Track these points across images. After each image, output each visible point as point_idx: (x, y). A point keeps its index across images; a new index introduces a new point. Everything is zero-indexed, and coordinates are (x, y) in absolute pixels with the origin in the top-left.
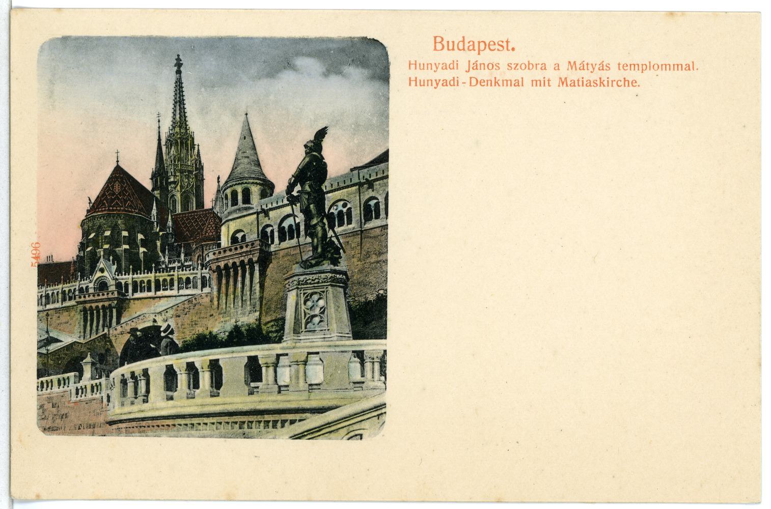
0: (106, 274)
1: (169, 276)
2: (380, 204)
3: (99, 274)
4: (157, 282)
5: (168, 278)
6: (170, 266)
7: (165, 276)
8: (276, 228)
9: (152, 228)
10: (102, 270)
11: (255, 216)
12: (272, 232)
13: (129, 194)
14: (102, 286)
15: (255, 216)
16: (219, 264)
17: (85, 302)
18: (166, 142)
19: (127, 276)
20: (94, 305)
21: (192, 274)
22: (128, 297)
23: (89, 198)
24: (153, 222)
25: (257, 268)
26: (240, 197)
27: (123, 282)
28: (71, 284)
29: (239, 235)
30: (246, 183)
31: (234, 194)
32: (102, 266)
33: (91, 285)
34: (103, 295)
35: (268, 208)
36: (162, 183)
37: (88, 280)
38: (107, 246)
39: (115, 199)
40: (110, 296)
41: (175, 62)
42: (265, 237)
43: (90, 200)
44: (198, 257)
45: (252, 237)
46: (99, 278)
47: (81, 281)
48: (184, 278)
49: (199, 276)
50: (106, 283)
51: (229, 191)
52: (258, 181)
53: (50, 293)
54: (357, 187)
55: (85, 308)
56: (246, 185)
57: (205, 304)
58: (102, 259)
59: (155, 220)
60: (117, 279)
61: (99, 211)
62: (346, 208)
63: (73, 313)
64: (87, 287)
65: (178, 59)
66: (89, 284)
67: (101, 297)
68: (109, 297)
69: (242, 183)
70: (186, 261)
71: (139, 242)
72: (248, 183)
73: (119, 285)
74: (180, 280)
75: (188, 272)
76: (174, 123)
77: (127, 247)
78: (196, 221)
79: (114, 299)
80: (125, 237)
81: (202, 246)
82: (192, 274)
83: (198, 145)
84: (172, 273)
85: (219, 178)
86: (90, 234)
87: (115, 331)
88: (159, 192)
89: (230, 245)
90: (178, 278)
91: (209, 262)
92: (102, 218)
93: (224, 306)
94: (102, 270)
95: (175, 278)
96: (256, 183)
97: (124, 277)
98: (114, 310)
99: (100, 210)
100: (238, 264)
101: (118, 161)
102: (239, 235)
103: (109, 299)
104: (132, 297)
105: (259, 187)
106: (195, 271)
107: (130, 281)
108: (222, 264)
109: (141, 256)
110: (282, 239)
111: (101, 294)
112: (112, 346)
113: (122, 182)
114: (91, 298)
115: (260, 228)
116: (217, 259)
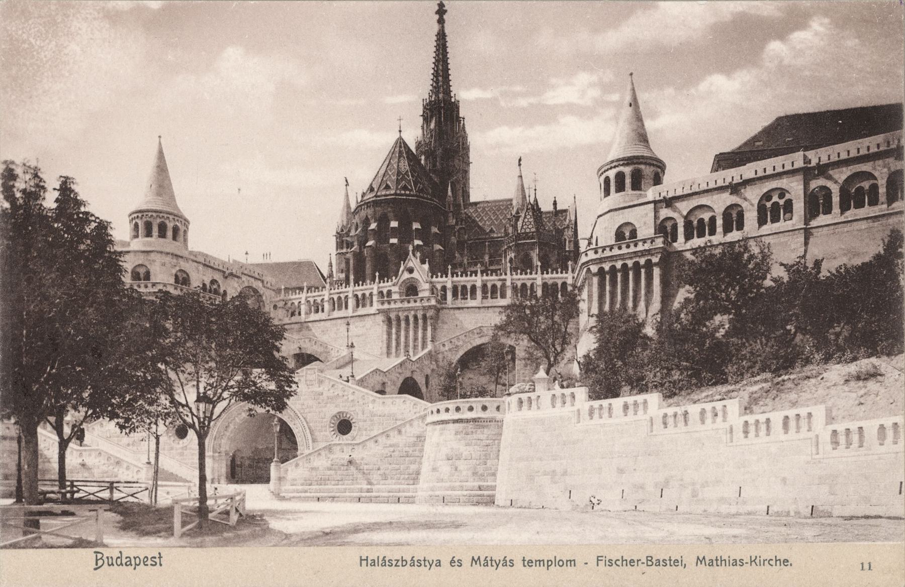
0: (415, 275)
1: (500, 280)
3: (406, 275)
4: (484, 286)
5: (499, 284)
6: (491, 268)
7: (494, 280)
9: (447, 220)
10: (411, 271)
11: (652, 205)
12: (675, 227)
13: (418, 175)
14: (411, 290)
15: (652, 205)
16: (603, 265)
18: (424, 112)
23: (347, 181)
25: (657, 272)
26: (628, 181)
28: (364, 287)
32: (410, 264)
33: (395, 289)
34: (415, 301)
37: (390, 283)
41: (437, 8)
43: (347, 181)
44: (511, 259)
45: (646, 230)
47: (380, 283)
48: (519, 284)
50: (416, 287)
51: (612, 174)
59: (452, 209)
60: (431, 283)
62: (771, 202)
64: (389, 293)
65: (441, 5)
66: (392, 286)
67: (412, 304)
70: (491, 263)
73: (433, 290)
76: (435, 87)
77: (420, 243)
78: (487, 213)
79: (430, 307)
83: (464, 118)
84: (503, 277)
85: (520, 160)
86: (370, 225)
94: (411, 271)
95: (508, 283)
97: (439, 279)
104: (451, 306)
106: (534, 276)
108: (607, 267)
110: (688, 237)
114: (399, 305)
116: (600, 259)
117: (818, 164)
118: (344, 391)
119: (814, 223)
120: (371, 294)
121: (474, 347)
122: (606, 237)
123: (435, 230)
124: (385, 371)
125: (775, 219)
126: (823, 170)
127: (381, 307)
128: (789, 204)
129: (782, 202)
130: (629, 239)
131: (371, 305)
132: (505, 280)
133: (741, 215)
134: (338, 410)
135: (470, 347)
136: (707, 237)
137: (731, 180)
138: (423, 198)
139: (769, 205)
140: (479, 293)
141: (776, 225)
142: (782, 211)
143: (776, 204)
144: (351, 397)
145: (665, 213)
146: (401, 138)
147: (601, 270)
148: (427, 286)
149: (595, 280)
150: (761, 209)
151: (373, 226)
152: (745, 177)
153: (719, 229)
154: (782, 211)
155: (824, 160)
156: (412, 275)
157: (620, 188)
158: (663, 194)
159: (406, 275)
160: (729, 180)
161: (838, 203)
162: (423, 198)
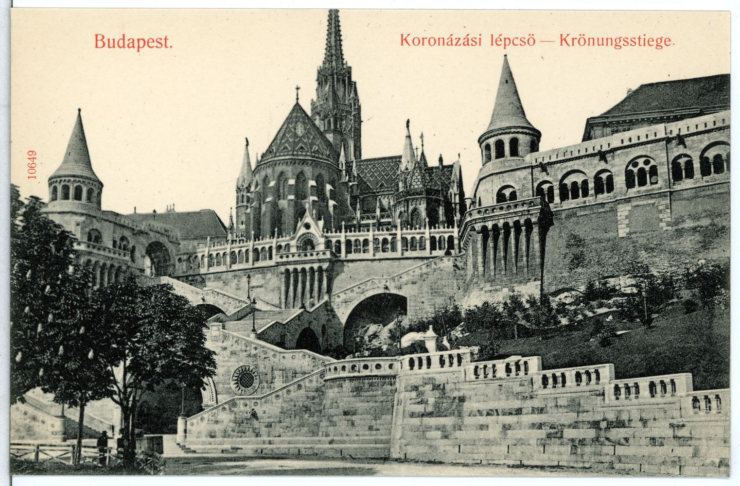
0: (312, 230)
1: (390, 234)
2: (694, 162)
3: (303, 230)
7: (386, 234)
8: (556, 185)
10: (307, 226)
12: (551, 189)
14: (308, 243)
15: (530, 170)
16: (486, 224)
17: (288, 263)
19: (338, 234)
20: (299, 267)
21: (438, 233)
22: (341, 259)
23: (247, 141)
24: (341, 171)
25: (536, 230)
27: (334, 240)
29: (507, 192)
30: (514, 132)
31: (500, 144)
33: (293, 243)
35: (545, 162)
36: (335, 124)
37: (288, 238)
38: (292, 197)
39: (299, 142)
40: (321, 257)
42: (543, 194)
43: (247, 141)
44: (401, 212)
46: (303, 234)
48: (409, 237)
49: (427, 236)
51: (492, 141)
52: (528, 131)
53: (237, 251)
54: (664, 142)
55: (287, 271)
56: (513, 135)
57: (447, 269)
58: (307, 213)
59: (344, 168)
60: (326, 237)
61: (280, 156)
63: (269, 276)
64: (288, 246)
67: (309, 258)
68: (320, 258)
69: (509, 133)
71: (328, 194)
72: (518, 133)
73: (328, 244)
74: (404, 239)
75: (413, 231)
77: (316, 198)
80: (312, 186)
81: (407, 201)
82: (438, 233)
83: (355, 83)
84: (394, 231)
85: (408, 122)
87: (336, 298)
88: (331, 135)
89: (495, 204)
90: (402, 238)
91: (471, 221)
92: (285, 164)
93: (492, 273)
94: (307, 226)
95: (399, 237)
96: (526, 133)
98: (325, 274)
99: (282, 154)
100: (511, 224)
101: (297, 99)
102: (507, 192)
103: (320, 261)
104: (345, 259)
105: (528, 138)
106: (422, 230)
107: (343, 240)
108: (490, 225)
109: (331, 209)
110: (564, 197)
111: (302, 254)
112: (334, 316)
113: (304, 123)
114: (296, 258)
115: (536, 185)
116: (484, 218)
117: (678, 135)
118: (247, 346)
119: (677, 187)
120: (270, 248)
121: (367, 299)
122: (489, 199)
123: (329, 187)
124: (284, 323)
125: (642, 183)
126: (681, 140)
127: (280, 260)
128: (654, 171)
129: (647, 168)
130: (510, 200)
131: (271, 258)
132: (396, 234)
133: (610, 179)
134: (241, 364)
135: (363, 298)
136: (581, 199)
137: (599, 148)
138: (318, 158)
139: (635, 170)
140: (371, 246)
141: (643, 188)
142: (648, 176)
143: (642, 171)
144: (253, 352)
145: (541, 176)
146: (297, 104)
147: (484, 228)
148: (322, 240)
149: (480, 237)
150: (629, 175)
151: (272, 184)
152: (612, 146)
153: (591, 192)
154: (648, 176)
155: (684, 132)
156: (308, 231)
157: (500, 154)
158: (540, 160)
159: (303, 230)
160: (598, 148)
161: (699, 169)
162: (318, 158)
